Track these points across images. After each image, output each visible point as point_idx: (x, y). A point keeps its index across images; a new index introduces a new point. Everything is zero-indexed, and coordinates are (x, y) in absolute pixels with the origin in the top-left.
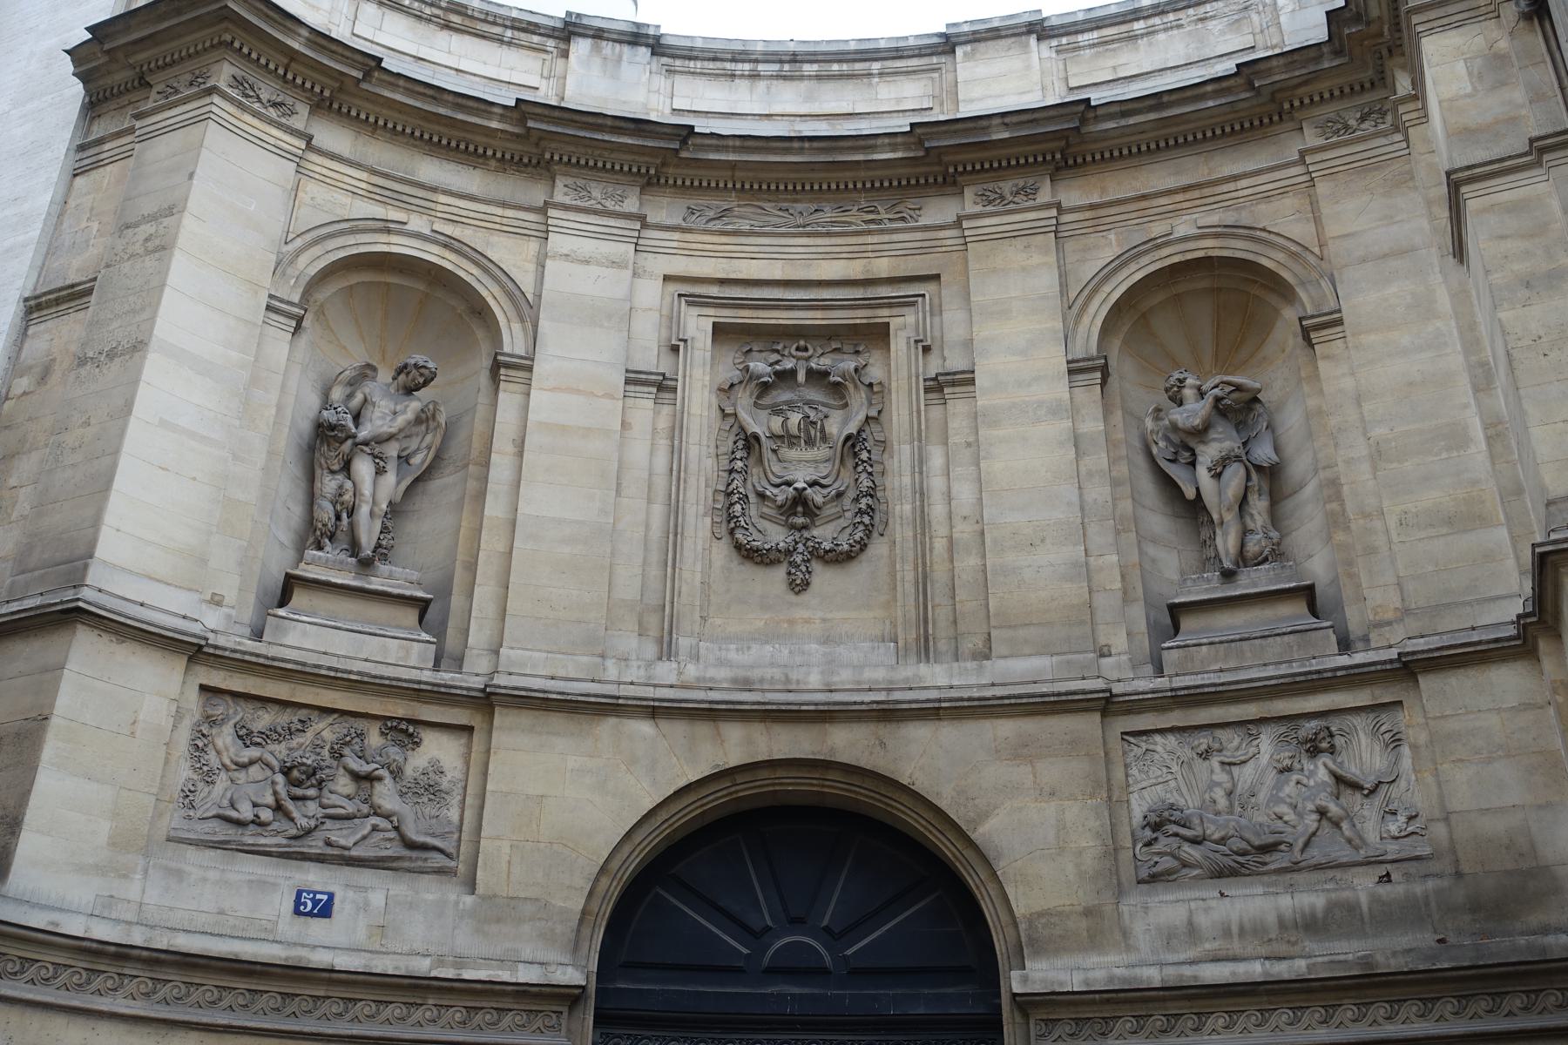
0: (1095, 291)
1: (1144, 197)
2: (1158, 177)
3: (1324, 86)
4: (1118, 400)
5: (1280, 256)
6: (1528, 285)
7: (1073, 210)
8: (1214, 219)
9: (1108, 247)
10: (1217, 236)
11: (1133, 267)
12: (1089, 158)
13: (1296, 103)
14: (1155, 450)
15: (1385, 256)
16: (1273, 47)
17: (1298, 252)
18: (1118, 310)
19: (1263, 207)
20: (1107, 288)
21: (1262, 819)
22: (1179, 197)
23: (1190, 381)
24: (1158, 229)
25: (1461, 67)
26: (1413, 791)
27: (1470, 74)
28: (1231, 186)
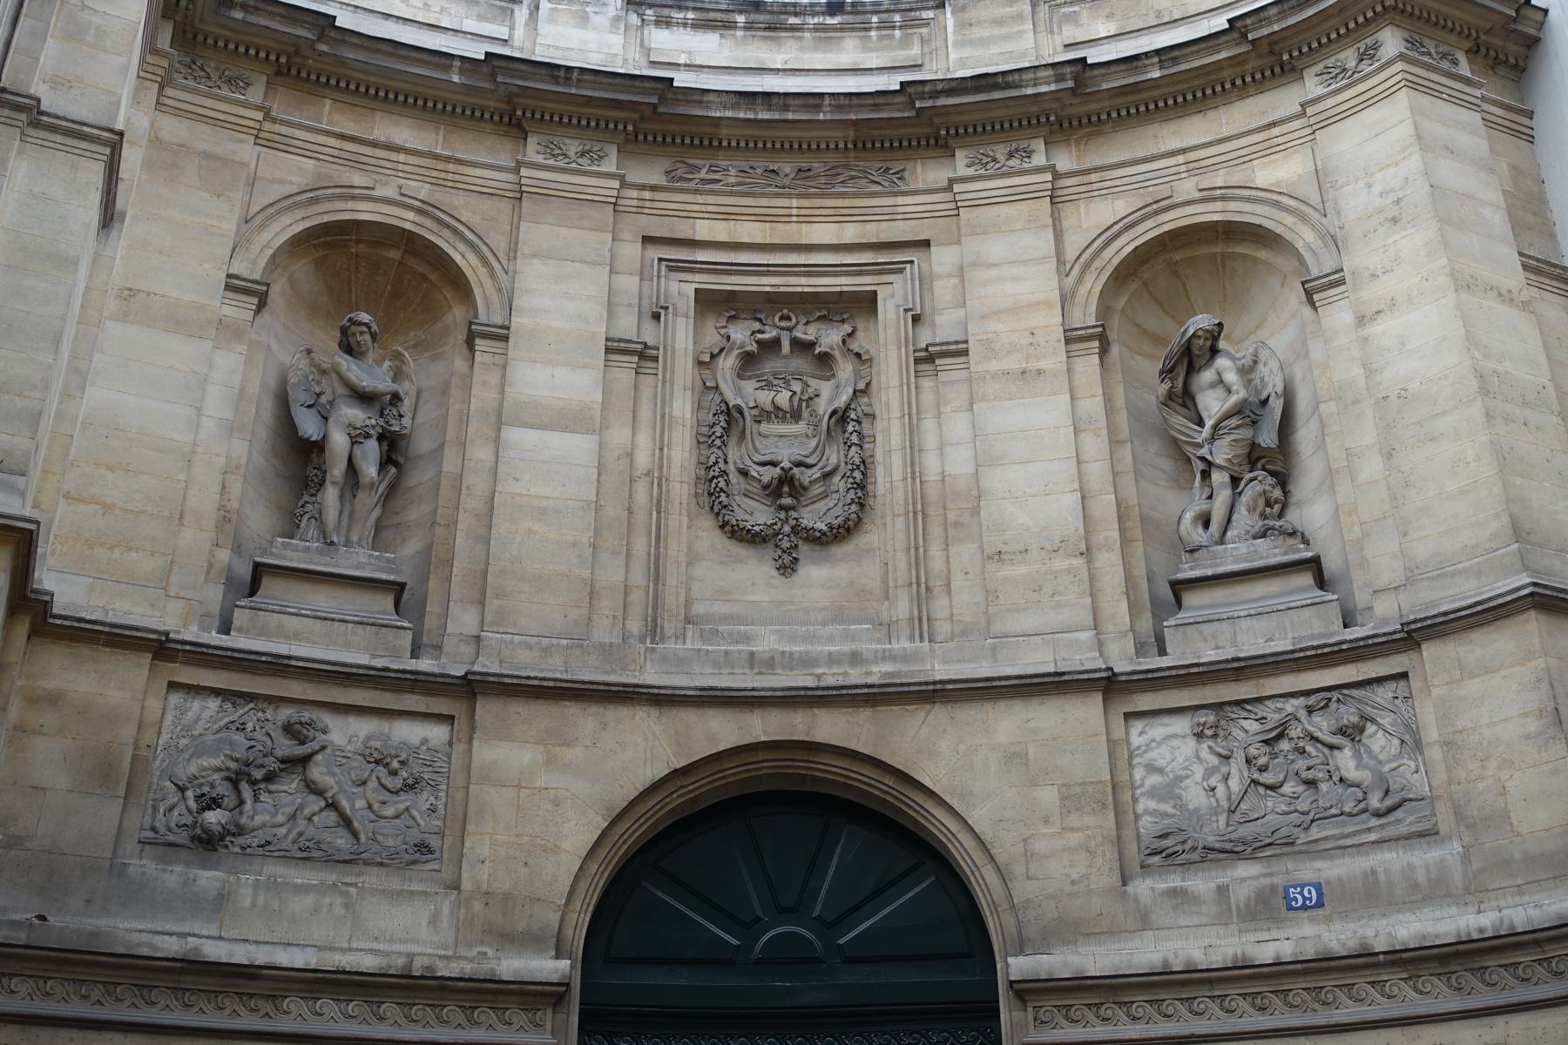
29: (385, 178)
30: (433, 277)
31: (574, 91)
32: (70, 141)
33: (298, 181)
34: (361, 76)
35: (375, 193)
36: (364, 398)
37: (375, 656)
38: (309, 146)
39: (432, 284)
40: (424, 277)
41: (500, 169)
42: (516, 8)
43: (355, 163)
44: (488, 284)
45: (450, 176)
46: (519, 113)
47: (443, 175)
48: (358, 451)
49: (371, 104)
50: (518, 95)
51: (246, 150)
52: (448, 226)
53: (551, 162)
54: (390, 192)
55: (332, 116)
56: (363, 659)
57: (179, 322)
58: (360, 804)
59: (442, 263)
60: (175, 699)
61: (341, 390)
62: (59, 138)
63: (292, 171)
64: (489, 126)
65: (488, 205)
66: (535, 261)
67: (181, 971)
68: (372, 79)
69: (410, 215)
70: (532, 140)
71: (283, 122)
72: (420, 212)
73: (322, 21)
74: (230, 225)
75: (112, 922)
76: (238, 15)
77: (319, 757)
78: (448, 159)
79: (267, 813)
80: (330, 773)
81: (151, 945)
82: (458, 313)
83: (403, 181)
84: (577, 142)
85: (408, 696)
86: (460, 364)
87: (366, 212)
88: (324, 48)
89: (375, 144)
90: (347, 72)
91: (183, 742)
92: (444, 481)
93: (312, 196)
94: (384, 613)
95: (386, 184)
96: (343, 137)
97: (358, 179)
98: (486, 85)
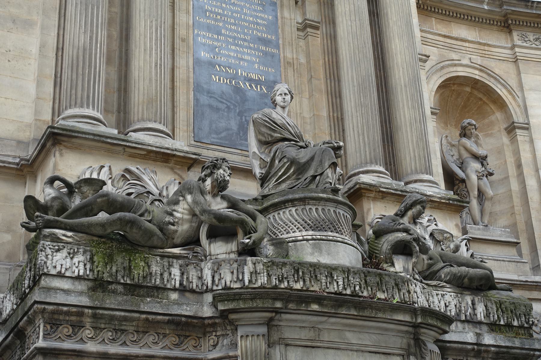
29: (463, 55)
30: (485, 99)
31: (534, 12)
34: (447, 7)
36: (476, 157)
37: (519, 276)
38: (433, 41)
39: (484, 102)
40: (481, 99)
43: (451, 48)
45: (487, 53)
47: (484, 52)
48: (481, 183)
49: (448, 19)
50: (510, 14)
52: (493, 77)
53: (525, 44)
54: (465, 61)
56: (515, 277)
61: (465, 155)
64: (496, 27)
66: (531, 92)
68: (451, 8)
69: (477, 72)
70: (515, 34)
72: (481, 70)
78: (485, 45)
82: (499, 115)
83: (470, 56)
84: (532, 34)
85: (534, 292)
86: (505, 140)
87: (462, 72)
89: (456, 39)
90: (442, 5)
92: (514, 195)
94: (514, 256)
95: (464, 57)
96: (445, 36)
97: (454, 56)
98: (498, 10)
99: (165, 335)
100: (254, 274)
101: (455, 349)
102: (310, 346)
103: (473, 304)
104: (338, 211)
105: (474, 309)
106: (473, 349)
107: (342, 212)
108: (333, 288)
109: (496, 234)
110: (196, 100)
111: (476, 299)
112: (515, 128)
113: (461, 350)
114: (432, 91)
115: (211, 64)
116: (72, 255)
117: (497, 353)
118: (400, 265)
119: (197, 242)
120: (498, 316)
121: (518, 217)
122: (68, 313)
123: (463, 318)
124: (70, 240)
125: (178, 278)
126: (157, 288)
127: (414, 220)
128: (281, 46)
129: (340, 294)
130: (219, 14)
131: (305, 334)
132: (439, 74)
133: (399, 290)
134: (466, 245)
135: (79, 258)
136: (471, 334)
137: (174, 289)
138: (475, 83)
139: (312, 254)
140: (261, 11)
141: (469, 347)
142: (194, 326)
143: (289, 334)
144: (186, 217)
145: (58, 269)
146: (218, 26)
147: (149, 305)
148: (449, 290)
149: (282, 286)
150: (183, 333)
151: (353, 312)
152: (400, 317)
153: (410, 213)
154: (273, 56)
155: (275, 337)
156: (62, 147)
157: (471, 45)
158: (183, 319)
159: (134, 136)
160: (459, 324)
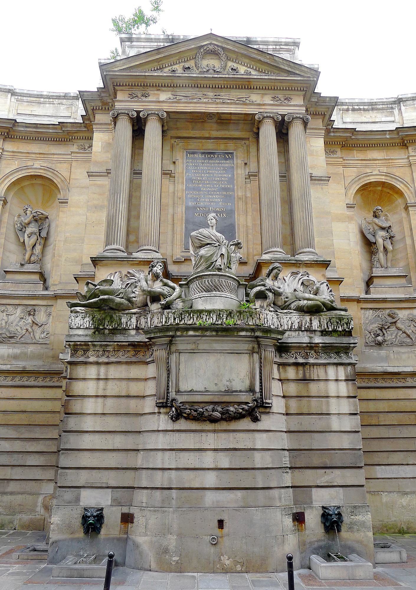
0: (8, 177)
1: (28, 153)
2: (35, 148)
3: (81, 135)
4: (8, 211)
5: (59, 180)
6: (96, 208)
7: (8, 151)
8: (45, 165)
9: (15, 165)
10: (45, 170)
11: (20, 173)
12: (15, 137)
13: (73, 138)
14: (16, 226)
15: (83, 187)
16: (75, 119)
17: (64, 180)
18: (14, 184)
19: (59, 165)
20: (11, 177)
21: (13, 330)
22: (38, 156)
23: (29, 209)
24: (30, 163)
25: (100, 144)
26: (48, 328)
27: (102, 146)
28: (52, 156)
30: (391, 192)
32: (319, 182)
33: (354, 175)
35: (374, 173)
40: (389, 193)
41: (403, 159)
42: (394, 111)
43: (366, 166)
44: (407, 191)
46: (406, 142)
49: (365, 149)
51: (341, 169)
55: (357, 155)
57: (339, 219)
58: (410, 331)
59: (393, 188)
60: (363, 311)
62: (317, 182)
63: (351, 173)
65: (402, 169)
67: (383, 374)
69: (383, 177)
71: (346, 160)
72: (386, 176)
73: (353, 130)
74: (343, 191)
75: (365, 365)
76: (332, 134)
77: (399, 321)
79: (390, 335)
80: (402, 325)
81: (376, 369)
87: (373, 179)
88: (353, 137)
89: (370, 160)
91: (367, 321)
93: (358, 177)
96: (362, 160)
97: (368, 171)
99: (128, 351)
100: (170, 318)
101: (295, 347)
102: (192, 352)
103: (311, 320)
104: (221, 279)
105: (311, 324)
106: (307, 346)
107: (223, 280)
108: (210, 321)
109: (393, 272)
110: (186, 228)
111: (313, 318)
112: (408, 207)
113: (299, 347)
114: (352, 194)
115: (195, 208)
116: (84, 318)
117: (322, 347)
118: (258, 303)
119: (147, 305)
120: (327, 326)
121: (410, 260)
122: (80, 345)
123: (303, 329)
124: (83, 311)
125: (135, 324)
126: (125, 329)
127: (276, 278)
128: (236, 190)
129: (214, 324)
130: (200, 180)
131: (190, 347)
132: (357, 183)
133: (253, 318)
134: (327, 285)
135: (87, 319)
136: (306, 338)
137: (133, 329)
138: (383, 184)
139: (202, 304)
140: (224, 174)
141: (304, 345)
142: (142, 346)
143: (181, 347)
144: (140, 293)
145: (77, 325)
146: (199, 187)
147: (120, 338)
148: (295, 314)
149: (181, 323)
150: (137, 349)
151: (214, 333)
152: (243, 333)
153: (272, 274)
154: (230, 196)
155: (173, 348)
156: (98, 266)
157: (380, 162)
158: (136, 343)
159: (135, 255)
160: (300, 332)
